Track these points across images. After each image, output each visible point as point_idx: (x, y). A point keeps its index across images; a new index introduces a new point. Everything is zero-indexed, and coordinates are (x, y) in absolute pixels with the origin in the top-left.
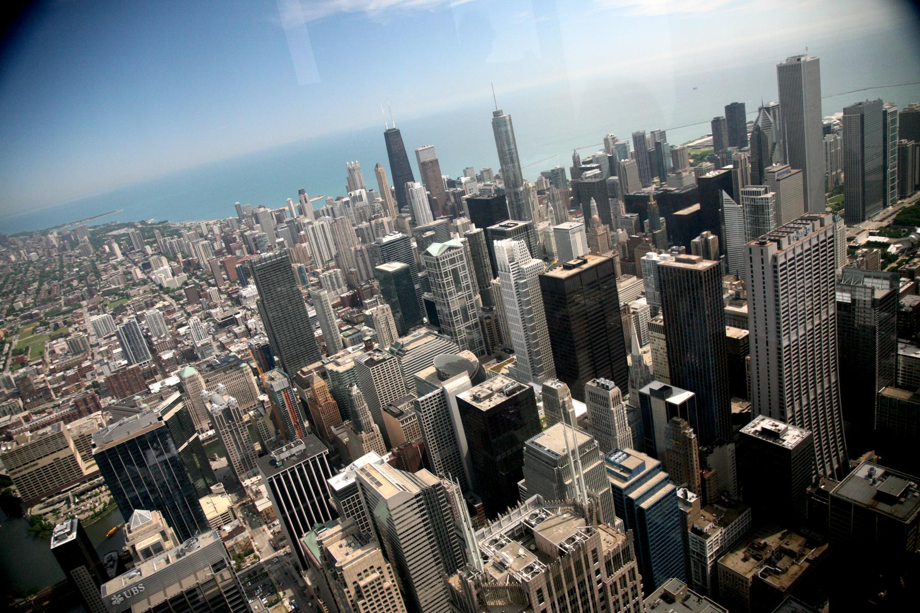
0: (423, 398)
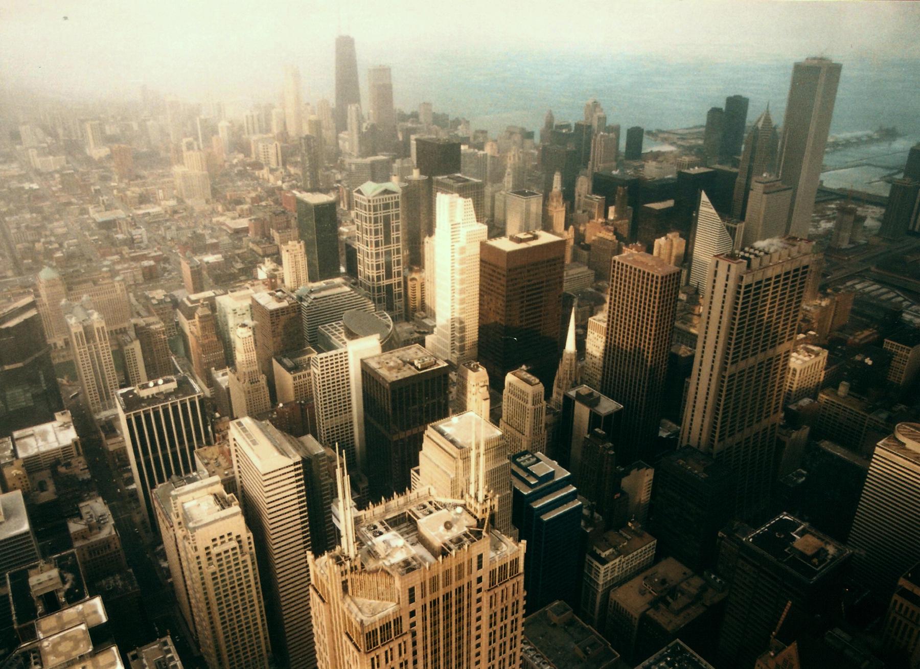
0: (323, 355)
